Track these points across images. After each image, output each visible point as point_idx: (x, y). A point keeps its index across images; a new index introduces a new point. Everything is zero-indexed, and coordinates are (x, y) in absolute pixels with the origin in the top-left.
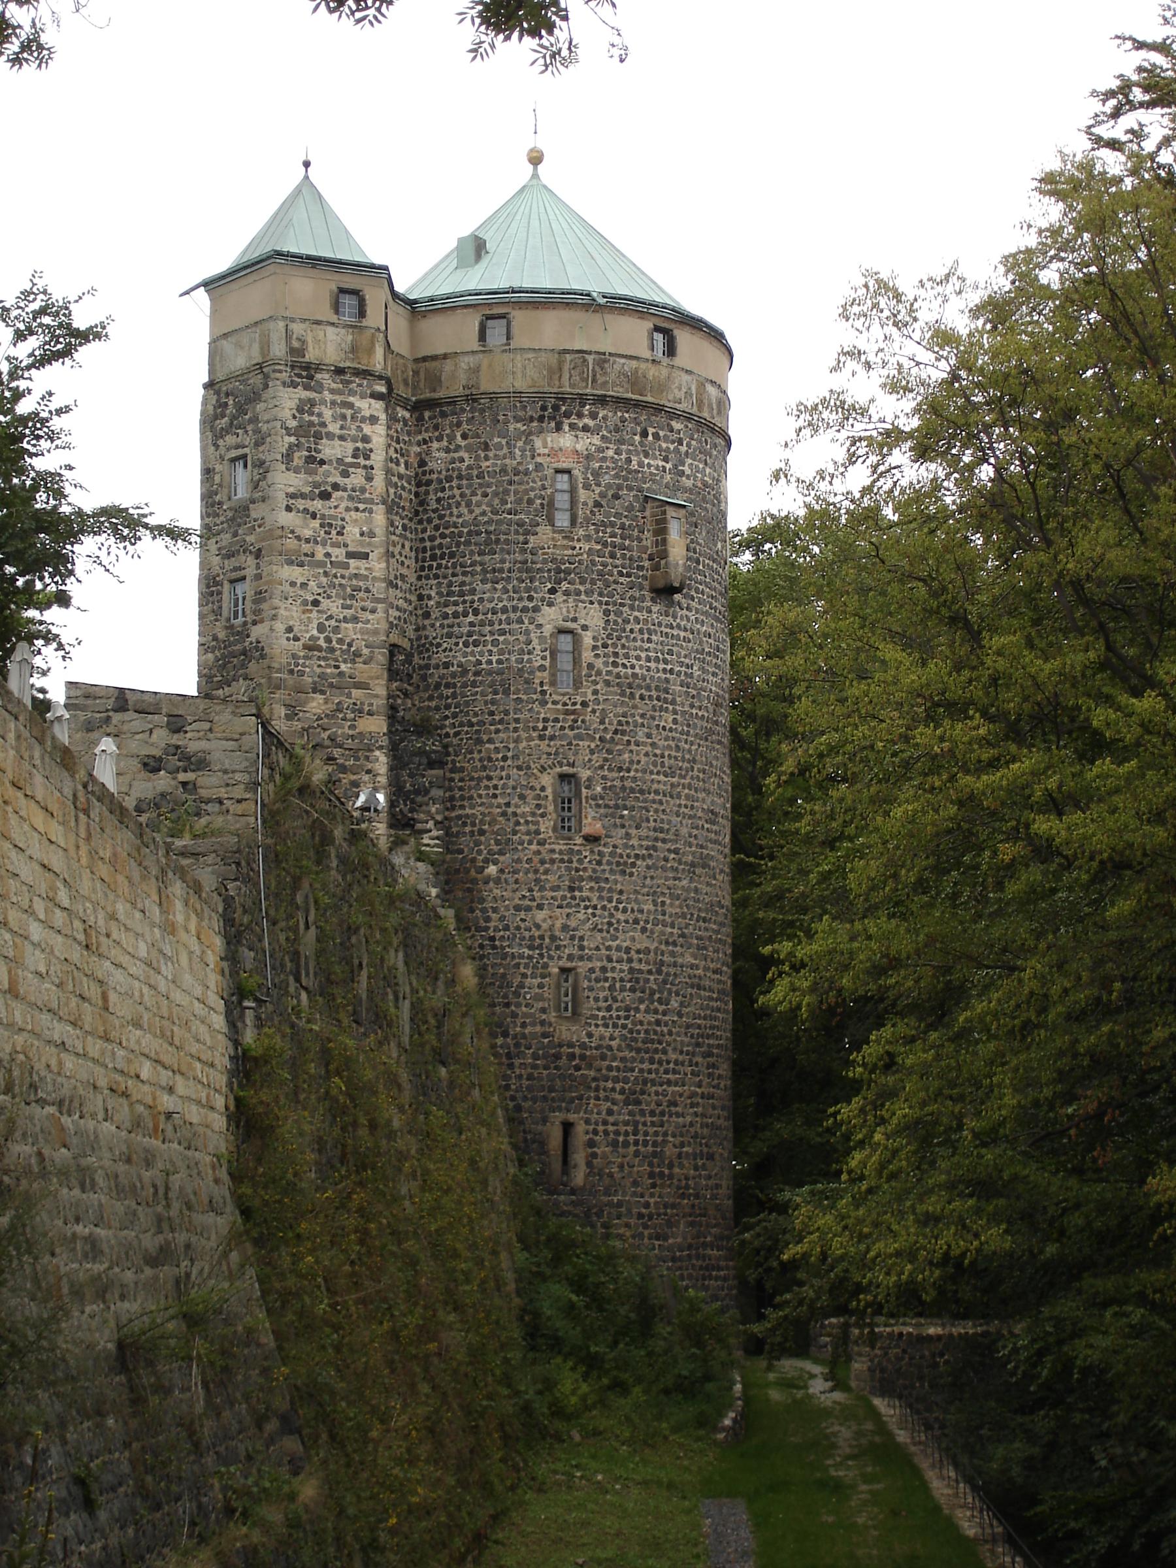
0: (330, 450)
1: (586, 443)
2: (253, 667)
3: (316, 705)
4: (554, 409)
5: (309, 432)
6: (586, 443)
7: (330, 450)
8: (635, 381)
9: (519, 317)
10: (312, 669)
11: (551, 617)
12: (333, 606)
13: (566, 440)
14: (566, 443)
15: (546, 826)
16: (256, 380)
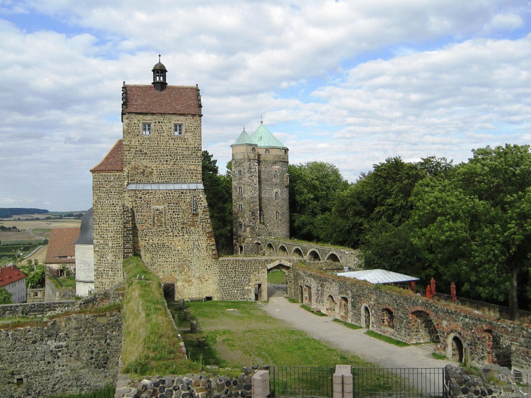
0: (253, 170)
1: (278, 167)
2: (243, 200)
3: (252, 205)
4: (275, 163)
5: (250, 168)
6: (278, 167)
7: (253, 170)
8: (283, 159)
9: (270, 150)
10: (251, 200)
11: (275, 191)
12: (253, 191)
13: (276, 167)
14: (276, 167)
15: (275, 218)
16: (243, 161)
